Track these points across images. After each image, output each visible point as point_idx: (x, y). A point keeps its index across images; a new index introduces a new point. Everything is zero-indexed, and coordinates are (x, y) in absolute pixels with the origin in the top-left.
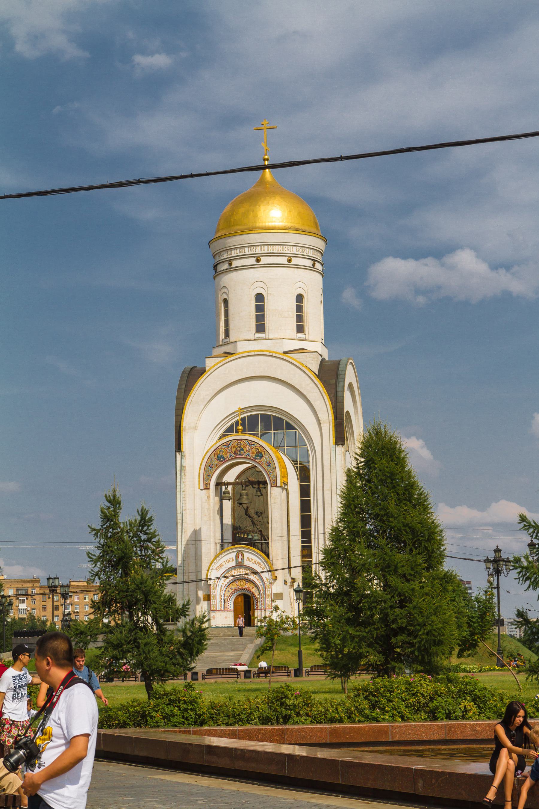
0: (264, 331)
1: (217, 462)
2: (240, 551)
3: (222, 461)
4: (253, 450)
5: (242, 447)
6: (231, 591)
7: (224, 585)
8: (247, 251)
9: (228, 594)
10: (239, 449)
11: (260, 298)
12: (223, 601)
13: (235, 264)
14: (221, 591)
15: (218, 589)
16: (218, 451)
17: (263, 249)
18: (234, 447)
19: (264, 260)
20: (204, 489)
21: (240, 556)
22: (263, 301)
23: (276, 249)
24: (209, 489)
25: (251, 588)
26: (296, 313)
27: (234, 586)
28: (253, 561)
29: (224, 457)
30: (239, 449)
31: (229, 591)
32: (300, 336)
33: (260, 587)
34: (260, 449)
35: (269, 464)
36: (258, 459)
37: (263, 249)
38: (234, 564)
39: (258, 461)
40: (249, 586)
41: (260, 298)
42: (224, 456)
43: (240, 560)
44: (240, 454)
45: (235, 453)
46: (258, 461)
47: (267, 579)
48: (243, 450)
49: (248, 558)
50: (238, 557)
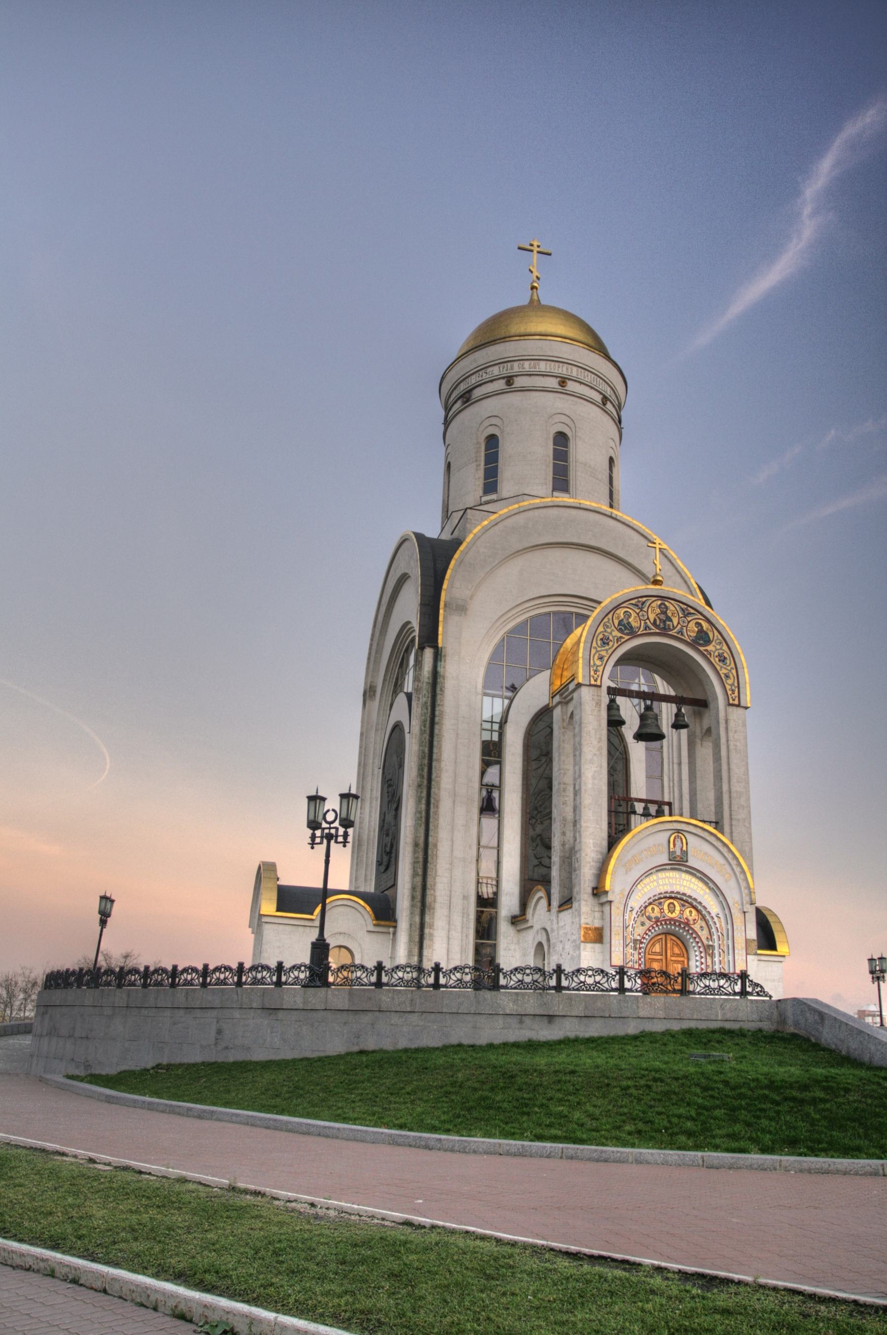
1: (617, 634)
2: (678, 831)
3: (627, 634)
4: (692, 625)
6: (648, 924)
7: (637, 909)
8: (543, 367)
9: (641, 930)
10: (663, 617)
11: (561, 439)
13: (519, 382)
16: (621, 612)
18: (653, 611)
19: (571, 386)
20: (590, 685)
21: (678, 843)
22: (566, 446)
24: (600, 686)
25: (691, 922)
29: (631, 627)
30: (663, 617)
31: (643, 924)
33: (716, 919)
34: (705, 625)
39: (702, 649)
40: (690, 914)
41: (561, 439)
42: (634, 624)
43: (678, 853)
44: (664, 628)
45: (654, 623)
46: (702, 649)
48: (671, 620)
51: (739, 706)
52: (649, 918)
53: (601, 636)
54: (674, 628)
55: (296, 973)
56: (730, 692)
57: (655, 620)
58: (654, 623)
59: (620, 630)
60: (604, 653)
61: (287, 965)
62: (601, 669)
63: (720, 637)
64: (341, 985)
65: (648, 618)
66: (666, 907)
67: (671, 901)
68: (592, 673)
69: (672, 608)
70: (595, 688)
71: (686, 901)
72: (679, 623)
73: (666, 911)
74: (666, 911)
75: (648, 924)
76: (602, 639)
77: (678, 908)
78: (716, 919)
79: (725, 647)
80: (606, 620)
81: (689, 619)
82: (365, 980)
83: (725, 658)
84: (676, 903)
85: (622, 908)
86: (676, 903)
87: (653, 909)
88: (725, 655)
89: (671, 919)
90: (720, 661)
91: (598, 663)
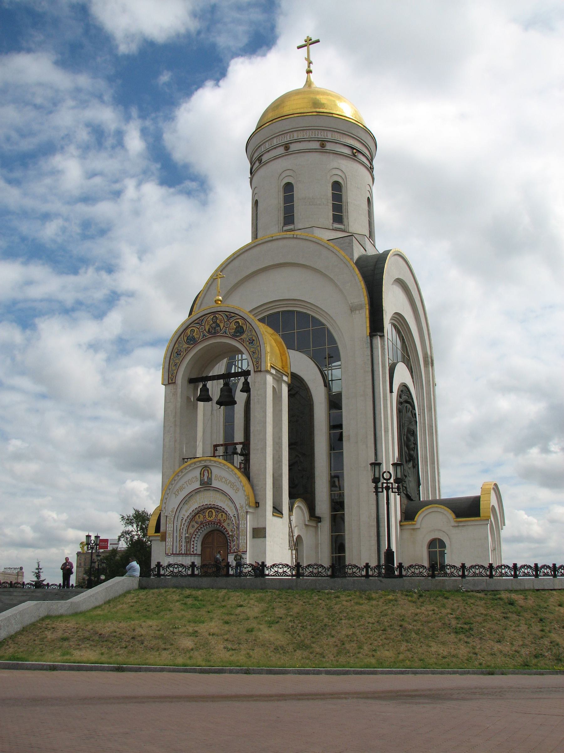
0: (293, 223)
2: (206, 466)
3: (192, 344)
5: (218, 322)
6: (196, 526)
9: (191, 530)
10: (214, 325)
11: (289, 187)
12: (184, 540)
13: (264, 158)
14: (181, 525)
15: (178, 524)
16: (189, 331)
17: (292, 136)
19: (293, 147)
21: (206, 474)
23: (307, 135)
26: (331, 202)
27: (200, 518)
28: (223, 480)
29: (194, 339)
31: (193, 526)
32: (337, 226)
35: (251, 341)
36: (237, 336)
37: (292, 136)
38: (197, 485)
39: (237, 339)
41: (289, 187)
43: (206, 480)
44: (215, 333)
45: (209, 332)
47: (242, 507)
49: (216, 476)
50: (204, 476)
51: (260, 371)
52: (197, 523)
53: (176, 351)
54: (221, 330)
55: (473, 570)
56: (255, 363)
57: (209, 329)
58: (209, 332)
59: (188, 343)
60: (177, 361)
61: (468, 565)
62: (175, 372)
63: (251, 327)
64: (411, 577)
65: (205, 329)
66: (207, 514)
67: (211, 510)
68: (170, 376)
69: (221, 317)
70: (172, 385)
71: (218, 510)
72: (224, 326)
73: (207, 517)
74: (207, 517)
75: (196, 526)
76: (176, 353)
77: (214, 514)
78: (233, 518)
79: (254, 333)
80: (180, 339)
81: (231, 321)
82: (324, 573)
83: (253, 340)
84: (213, 511)
85: (172, 519)
86: (213, 511)
87: (199, 517)
88: (254, 338)
89: (210, 521)
90: (250, 343)
91: (174, 368)
